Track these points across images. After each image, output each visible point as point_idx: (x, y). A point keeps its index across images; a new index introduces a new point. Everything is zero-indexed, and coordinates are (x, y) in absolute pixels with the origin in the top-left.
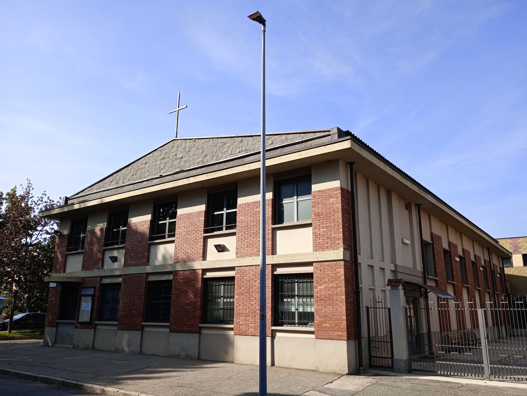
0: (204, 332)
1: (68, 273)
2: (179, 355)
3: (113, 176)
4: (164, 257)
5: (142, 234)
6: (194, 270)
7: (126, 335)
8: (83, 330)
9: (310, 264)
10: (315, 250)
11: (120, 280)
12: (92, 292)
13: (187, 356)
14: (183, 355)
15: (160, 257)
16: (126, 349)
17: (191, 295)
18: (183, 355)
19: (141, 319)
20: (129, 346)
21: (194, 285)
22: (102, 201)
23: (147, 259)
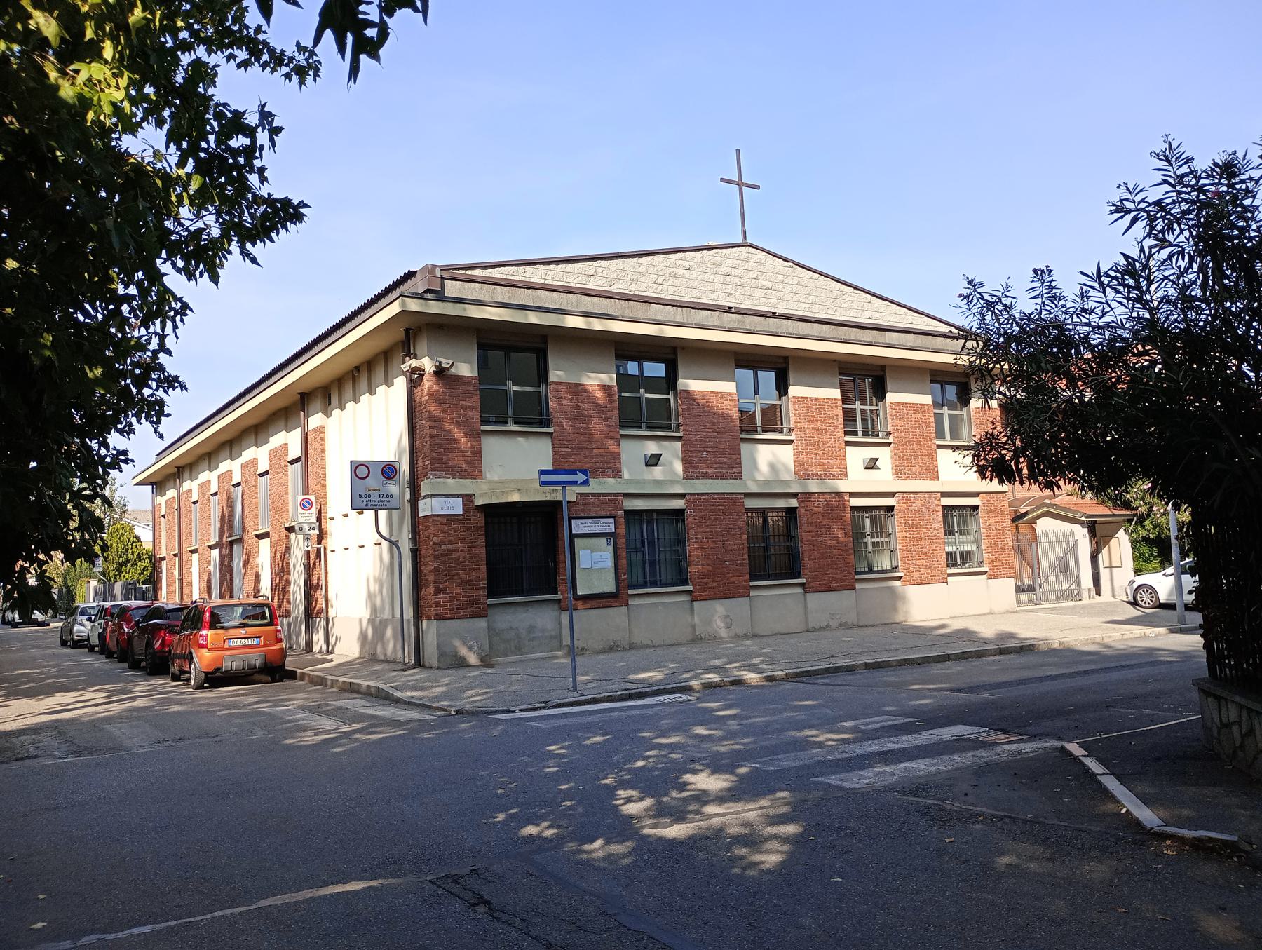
0: (858, 586)
1: (629, 482)
2: (828, 626)
3: (595, 263)
4: (772, 466)
5: (724, 417)
6: (837, 493)
7: (719, 608)
8: (594, 613)
9: (977, 494)
10: (356, 466)
11: (679, 504)
12: (609, 526)
13: (841, 625)
14: (834, 624)
15: (763, 467)
16: (723, 633)
17: (839, 533)
18: (834, 624)
19: (748, 576)
20: (728, 627)
21: (841, 517)
22: (589, 323)
23: (732, 466)
